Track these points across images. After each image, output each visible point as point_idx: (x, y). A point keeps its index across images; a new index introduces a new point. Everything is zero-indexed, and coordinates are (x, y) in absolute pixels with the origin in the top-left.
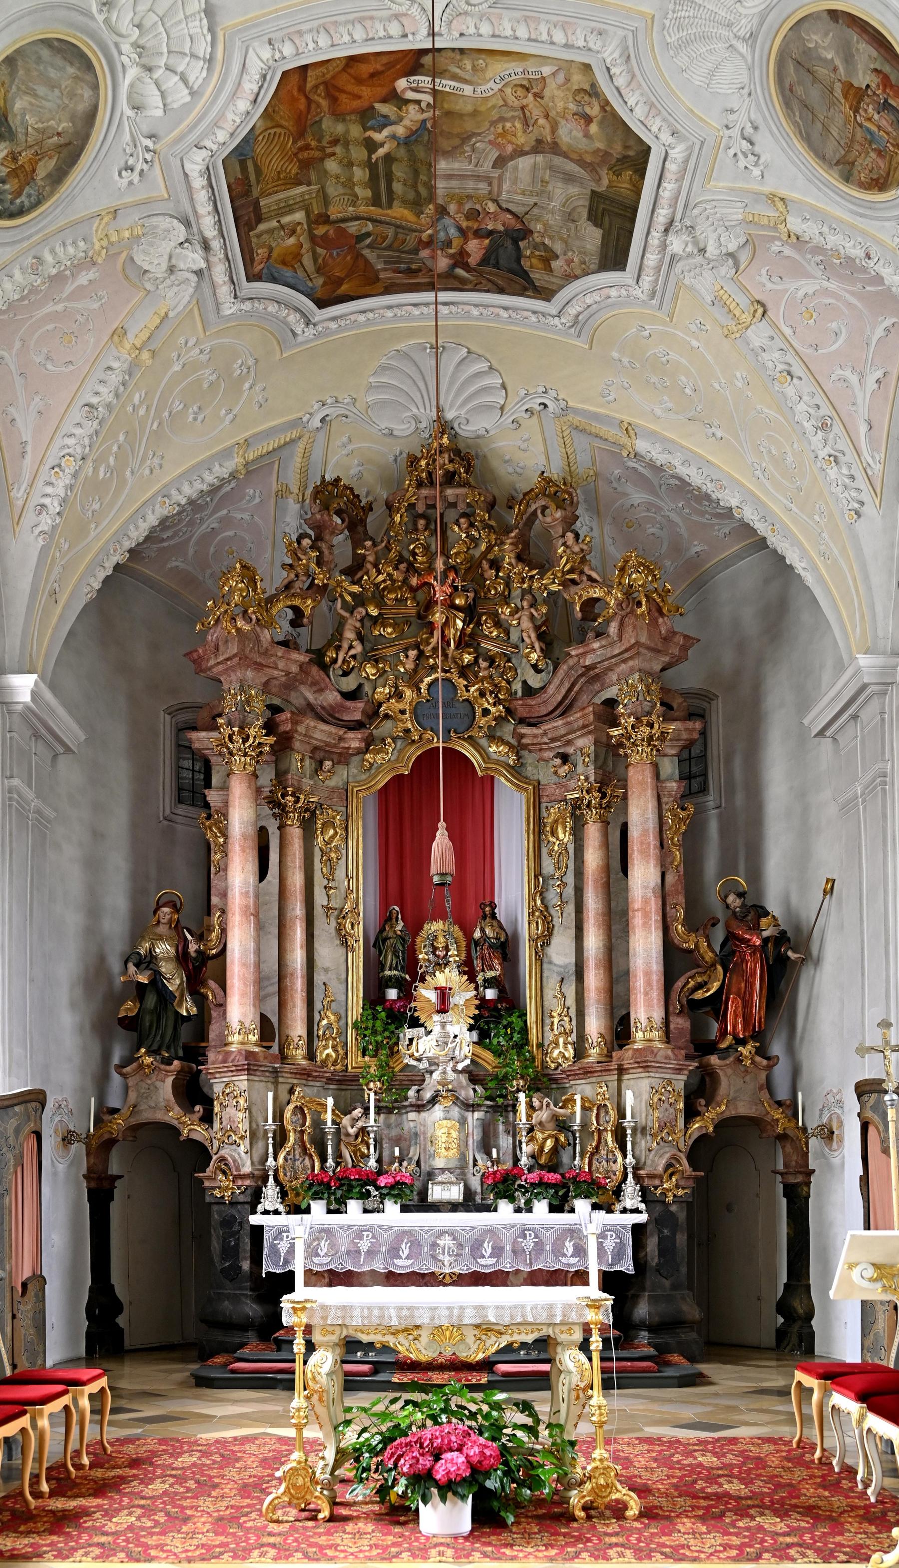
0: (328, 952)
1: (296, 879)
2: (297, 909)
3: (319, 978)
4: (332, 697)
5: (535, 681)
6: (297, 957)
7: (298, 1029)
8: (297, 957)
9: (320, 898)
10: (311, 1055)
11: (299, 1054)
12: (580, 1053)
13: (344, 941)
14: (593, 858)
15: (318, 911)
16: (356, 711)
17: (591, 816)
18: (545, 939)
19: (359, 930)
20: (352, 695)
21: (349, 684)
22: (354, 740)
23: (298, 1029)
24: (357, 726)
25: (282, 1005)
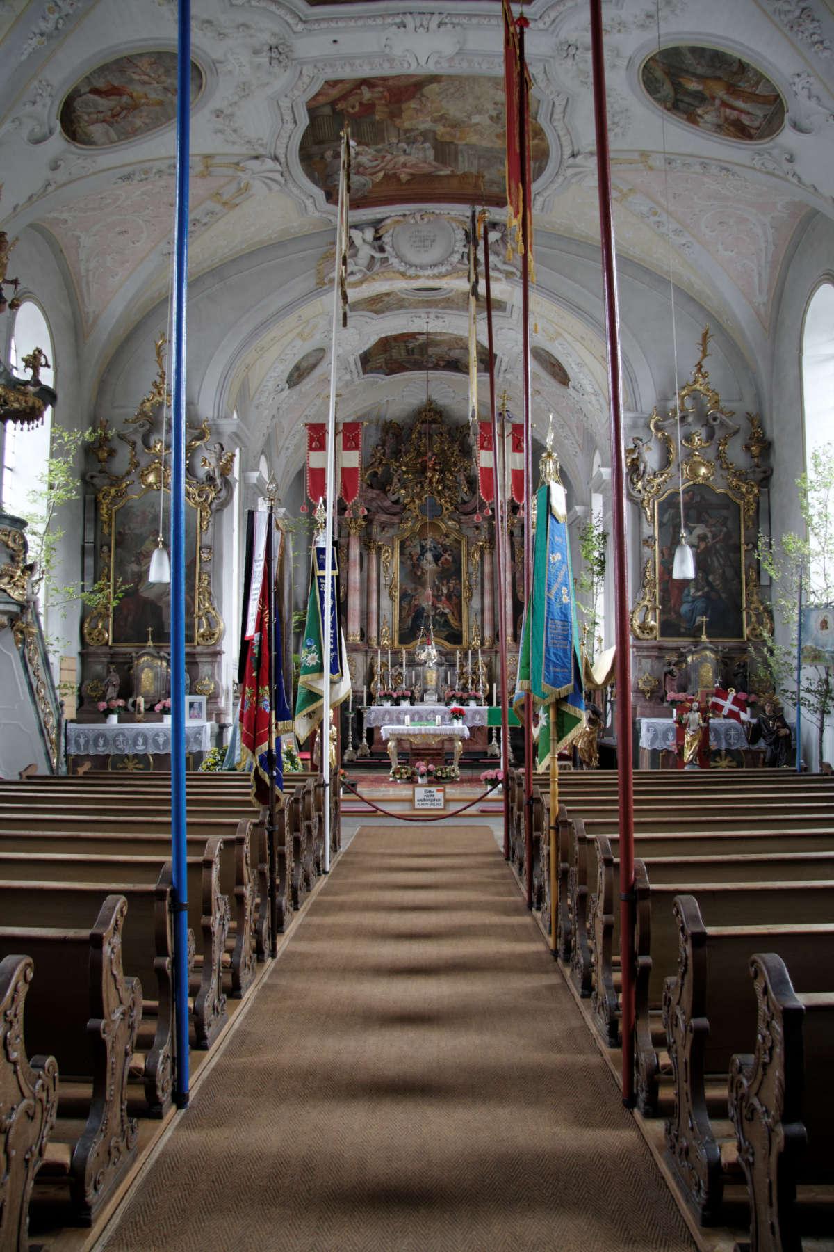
0: (386, 603)
1: (374, 575)
2: (374, 587)
3: (382, 613)
4: (387, 504)
5: (466, 498)
6: (374, 605)
7: (374, 634)
8: (374, 605)
9: (382, 581)
10: (379, 644)
11: (374, 644)
12: (482, 644)
13: (392, 598)
14: (487, 568)
15: (382, 587)
16: (397, 509)
17: (487, 552)
18: (470, 598)
19: (398, 594)
20: (396, 502)
21: (394, 498)
22: (396, 520)
23: (374, 634)
24: (395, 514)
25: (368, 624)
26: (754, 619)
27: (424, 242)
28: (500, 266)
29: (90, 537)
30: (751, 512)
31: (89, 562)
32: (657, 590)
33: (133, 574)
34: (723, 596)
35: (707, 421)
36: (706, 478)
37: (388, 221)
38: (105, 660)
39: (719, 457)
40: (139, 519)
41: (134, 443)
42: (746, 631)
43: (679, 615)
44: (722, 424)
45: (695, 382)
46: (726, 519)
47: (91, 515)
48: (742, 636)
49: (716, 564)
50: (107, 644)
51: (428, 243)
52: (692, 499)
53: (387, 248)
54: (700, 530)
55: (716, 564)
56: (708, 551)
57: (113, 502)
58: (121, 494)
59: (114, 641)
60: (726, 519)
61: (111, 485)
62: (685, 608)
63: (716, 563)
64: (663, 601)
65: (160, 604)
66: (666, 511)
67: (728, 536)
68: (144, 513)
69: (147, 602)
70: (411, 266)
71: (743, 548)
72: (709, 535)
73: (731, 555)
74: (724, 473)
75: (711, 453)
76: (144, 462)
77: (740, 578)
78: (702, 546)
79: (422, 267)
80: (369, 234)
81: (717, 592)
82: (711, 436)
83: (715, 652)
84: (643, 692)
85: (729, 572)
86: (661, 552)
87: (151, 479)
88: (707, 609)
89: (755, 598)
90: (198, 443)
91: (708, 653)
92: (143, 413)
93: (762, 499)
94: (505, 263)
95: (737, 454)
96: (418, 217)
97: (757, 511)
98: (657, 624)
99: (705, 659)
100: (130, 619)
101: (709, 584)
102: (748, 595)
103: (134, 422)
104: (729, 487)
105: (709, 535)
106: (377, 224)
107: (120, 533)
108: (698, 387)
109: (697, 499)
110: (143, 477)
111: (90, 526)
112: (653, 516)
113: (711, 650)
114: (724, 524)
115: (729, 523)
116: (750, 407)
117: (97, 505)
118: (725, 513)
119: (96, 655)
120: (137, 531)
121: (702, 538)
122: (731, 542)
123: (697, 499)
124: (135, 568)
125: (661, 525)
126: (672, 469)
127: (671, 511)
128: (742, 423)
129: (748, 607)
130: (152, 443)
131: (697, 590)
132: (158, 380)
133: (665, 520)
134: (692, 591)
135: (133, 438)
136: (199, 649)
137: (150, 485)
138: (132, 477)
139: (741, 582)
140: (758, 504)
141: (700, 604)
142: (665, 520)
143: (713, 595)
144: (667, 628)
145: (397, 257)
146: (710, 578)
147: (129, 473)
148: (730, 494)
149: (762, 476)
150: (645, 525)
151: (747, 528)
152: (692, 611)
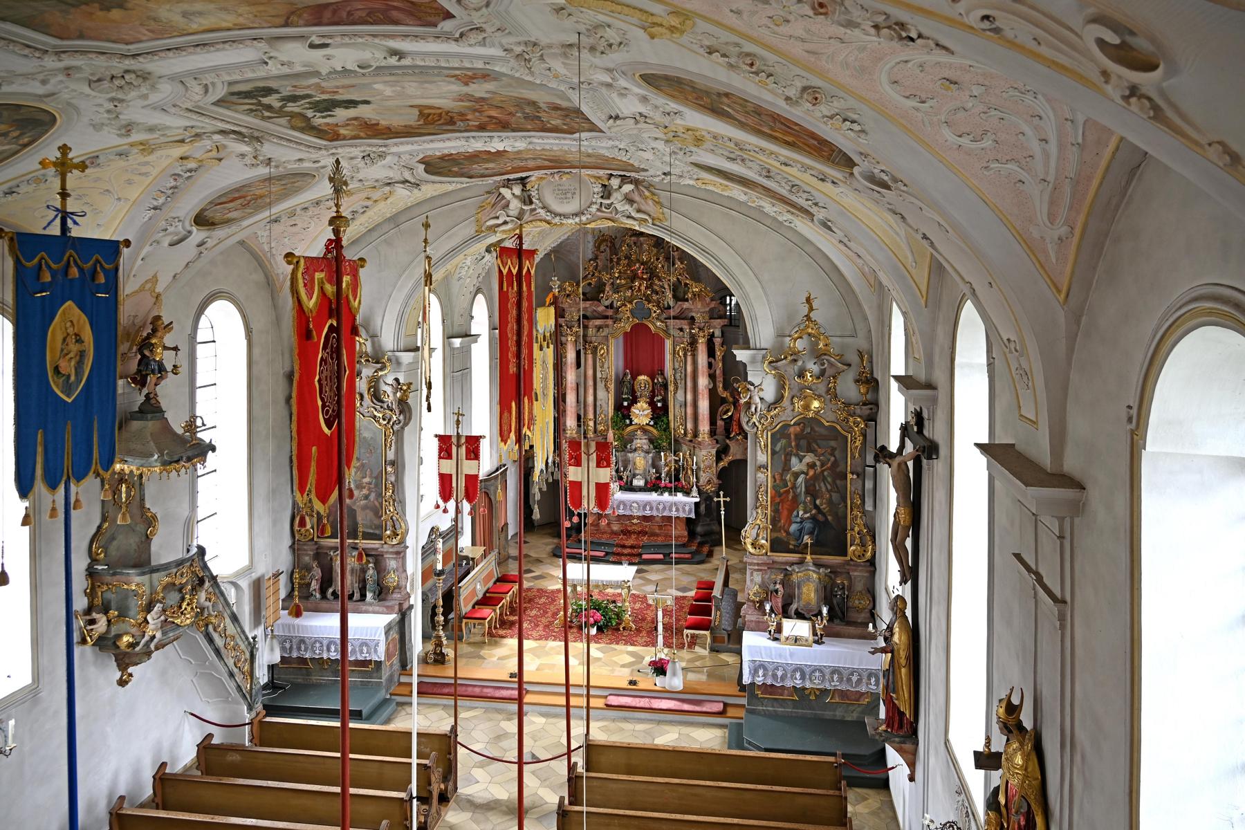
27: (564, 195)
28: (633, 214)
30: (858, 443)
32: (769, 512)
36: (817, 413)
37: (533, 179)
43: (788, 533)
46: (834, 449)
48: (846, 555)
51: (569, 195)
52: (803, 430)
54: (809, 458)
60: (834, 449)
62: (793, 528)
64: (774, 521)
66: (779, 440)
67: (835, 464)
70: (556, 215)
71: (850, 476)
72: (818, 463)
73: (838, 482)
75: (822, 389)
78: (811, 473)
79: (566, 216)
80: (517, 190)
81: (824, 515)
83: (818, 573)
84: (753, 602)
85: (835, 496)
86: (774, 477)
88: (814, 529)
89: (859, 521)
93: (870, 432)
94: (639, 211)
95: (849, 388)
101: (816, 507)
102: (852, 519)
105: (818, 463)
106: (522, 179)
109: (808, 430)
112: (766, 446)
114: (832, 454)
115: (837, 453)
118: (833, 443)
121: (811, 466)
122: (838, 470)
123: (808, 430)
125: (774, 453)
127: (784, 441)
131: (805, 512)
134: (801, 513)
140: (865, 436)
141: (808, 525)
142: (777, 449)
143: (820, 517)
144: (777, 545)
145: (543, 208)
146: (818, 502)
150: (759, 452)
151: (853, 457)
152: (800, 530)
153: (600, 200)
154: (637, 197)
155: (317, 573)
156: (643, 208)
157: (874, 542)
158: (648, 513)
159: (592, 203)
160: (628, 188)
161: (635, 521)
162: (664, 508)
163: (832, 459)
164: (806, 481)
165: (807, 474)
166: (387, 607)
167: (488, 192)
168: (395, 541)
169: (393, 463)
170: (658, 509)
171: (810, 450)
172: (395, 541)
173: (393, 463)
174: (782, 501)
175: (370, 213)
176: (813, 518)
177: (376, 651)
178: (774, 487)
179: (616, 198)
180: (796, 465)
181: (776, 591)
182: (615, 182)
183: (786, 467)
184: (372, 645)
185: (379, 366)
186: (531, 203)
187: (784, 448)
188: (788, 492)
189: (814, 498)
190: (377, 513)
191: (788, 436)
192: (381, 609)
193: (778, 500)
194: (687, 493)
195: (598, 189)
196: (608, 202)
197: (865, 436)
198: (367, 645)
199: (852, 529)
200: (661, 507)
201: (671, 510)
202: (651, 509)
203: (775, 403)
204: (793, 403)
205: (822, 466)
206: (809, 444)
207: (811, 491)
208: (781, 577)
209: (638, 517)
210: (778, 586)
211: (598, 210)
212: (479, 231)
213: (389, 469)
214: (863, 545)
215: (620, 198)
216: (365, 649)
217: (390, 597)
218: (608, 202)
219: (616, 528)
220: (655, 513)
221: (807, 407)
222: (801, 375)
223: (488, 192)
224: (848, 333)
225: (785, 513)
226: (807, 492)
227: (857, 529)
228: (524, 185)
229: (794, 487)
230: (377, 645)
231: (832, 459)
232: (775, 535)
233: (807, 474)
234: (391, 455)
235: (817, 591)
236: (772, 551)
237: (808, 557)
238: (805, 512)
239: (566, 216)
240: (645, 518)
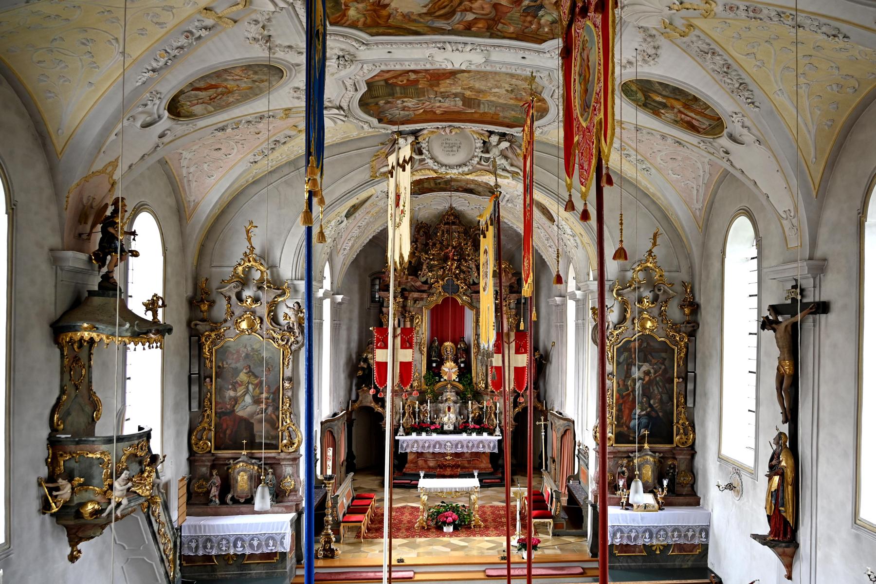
26: (681, 431)
27: (451, 148)
28: (508, 168)
29: (195, 370)
30: (682, 355)
31: (195, 389)
32: (614, 411)
33: (231, 398)
34: (660, 414)
35: (654, 286)
37: (425, 132)
38: (209, 464)
39: (661, 313)
40: (235, 356)
41: (230, 298)
42: (676, 439)
43: (628, 427)
44: (665, 291)
45: (647, 261)
46: (665, 359)
47: (195, 352)
48: (672, 443)
49: (656, 392)
50: (210, 452)
51: (455, 149)
53: (424, 151)
54: (645, 367)
55: (656, 392)
56: (650, 382)
57: (214, 343)
58: (219, 337)
59: (216, 449)
60: (665, 359)
61: (212, 330)
63: (656, 391)
65: (252, 421)
67: (665, 371)
68: (238, 352)
69: (242, 419)
70: (442, 165)
71: (676, 380)
72: (652, 371)
73: (667, 385)
74: (664, 326)
75: (656, 312)
76: (237, 313)
77: (673, 401)
78: (647, 379)
79: (451, 167)
81: (656, 412)
82: (655, 299)
83: (654, 457)
85: (665, 397)
86: (618, 383)
87: (244, 325)
88: (648, 423)
89: (682, 416)
90: (280, 299)
91: (648, 457)
92: (235, 275)
94: (512, 165)
95: (675, 312)
96: (448, 130)
97: (686, 355)
98: (613, 436)
99: (647, 462)
100: (228, 432)
101: (651, 406)
102: (677, 414)
103: (229, 282)
104: (667, 336)
105: (652, 371)
106: (415, 133)
107: (219, 367)
108: (649, 264)
109: (645, 345)
110: (237, 323)
111: (195, 362)
112: (613, 358)
113: (651, 456)
114: (663, 364)
115: (666, 362)
116: (684, 276)
117: (200, 347)
118: (663, 355)
119: (203, 461)
120: (233, 366)
121: (647, 373)
122: (667, 376)
123: (645, 345)
124: (232, 393)
125: (618, 364)
126: (628, 323)
127: (626, 354)
128: (679, 288)
129: (677, 422)
130: (244, 297)
131: (642, 410)
132: (248, 251)
133: (621, 360)
135: (228, 294)
136: (283, 455)
137: (243, 331)
138: (228, 324)
139: (673, 405)
140: (687, 348)
143: (653, 414)
146: (652, 402)
147: (226, 321)
148: (668, 342)
149: (691, 329)
151: (678, 366)
153: (481, 154)
154: (510, 155)
155: (217, 480)
156: (515, 163)
157: (694, 432)
158: (459, 450)
159: (474, 156)
160: (505, 145)
161: (448, 458)
162: (473, 446)
163: (663, 367)
164: (643, 385)
165: (643, 380)
166: (286, 507)
167: (382, 144)
168: (291, 450)
169: (290, 380)
170: (468, 447)
171: (645, 360)
172: (291, 450)
173: (290, 380)
174: (624, 402)
175: (276, 154)
176: (648, 414)
177: (282, 543)
178: (618, 391)
179: (494, 153)
180: (636, 373)
181: (623, 473)
182: (494, 139)
183: (628, 374)
184: (278, 538)
185: (279, 292)
186: (420, 153)
187: (626, 360)
188: (629, 395)
189: (649, 399)
190: (273, 423)
191: (629, 350)
192: (280, 509)
193: (621, 401)
194: (491, 433)
195: (479, 144)
196: (487, 156)
197: (687, 348)
198: (273, 539)
199: (677, 422)
200: (470, 445)
201: (478, 447)
202: (462, 447)
203: (618, 324)
204: (633, 323)
205: (655, 373)
206: (646, 356)
207: (646, 393)
208: (625, 461)
209: (451, 454)
210: (624, 469)
211: (478, 163)
212: (374, 177)
213: (287, 385)
214: (686, 434)
215: (497, 153)
216: (271, 543)
217: (286, 499)
218: (487, 156)
219: (432, 464)
220: (465, 450)
221: (644, 327)
222: (640, 301)
223: (382, 144)
224: (674, 269)
225: (627, 412)
226: (644, 395)
227: (681, 422)
228: (416, 138)
229: (634, 390)
230: (283, 538)
231: (663, 367)
232: (619, 429)
233: (643, 380)
234: (288, 373)
235: (653, 471)
236: (616, 443)
237: (646, 446)
238: (642, 410)
239: (451, 167)
240: (457, 455)
